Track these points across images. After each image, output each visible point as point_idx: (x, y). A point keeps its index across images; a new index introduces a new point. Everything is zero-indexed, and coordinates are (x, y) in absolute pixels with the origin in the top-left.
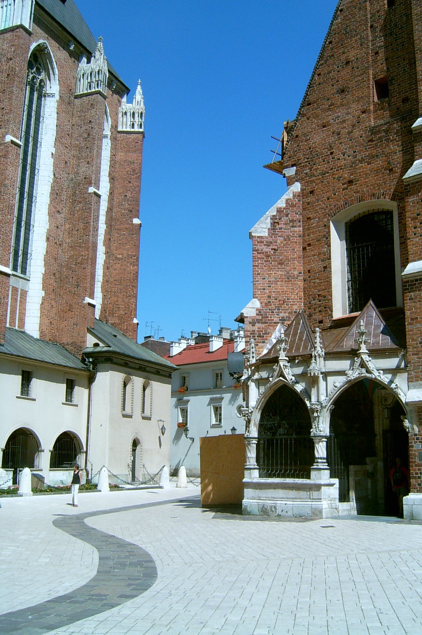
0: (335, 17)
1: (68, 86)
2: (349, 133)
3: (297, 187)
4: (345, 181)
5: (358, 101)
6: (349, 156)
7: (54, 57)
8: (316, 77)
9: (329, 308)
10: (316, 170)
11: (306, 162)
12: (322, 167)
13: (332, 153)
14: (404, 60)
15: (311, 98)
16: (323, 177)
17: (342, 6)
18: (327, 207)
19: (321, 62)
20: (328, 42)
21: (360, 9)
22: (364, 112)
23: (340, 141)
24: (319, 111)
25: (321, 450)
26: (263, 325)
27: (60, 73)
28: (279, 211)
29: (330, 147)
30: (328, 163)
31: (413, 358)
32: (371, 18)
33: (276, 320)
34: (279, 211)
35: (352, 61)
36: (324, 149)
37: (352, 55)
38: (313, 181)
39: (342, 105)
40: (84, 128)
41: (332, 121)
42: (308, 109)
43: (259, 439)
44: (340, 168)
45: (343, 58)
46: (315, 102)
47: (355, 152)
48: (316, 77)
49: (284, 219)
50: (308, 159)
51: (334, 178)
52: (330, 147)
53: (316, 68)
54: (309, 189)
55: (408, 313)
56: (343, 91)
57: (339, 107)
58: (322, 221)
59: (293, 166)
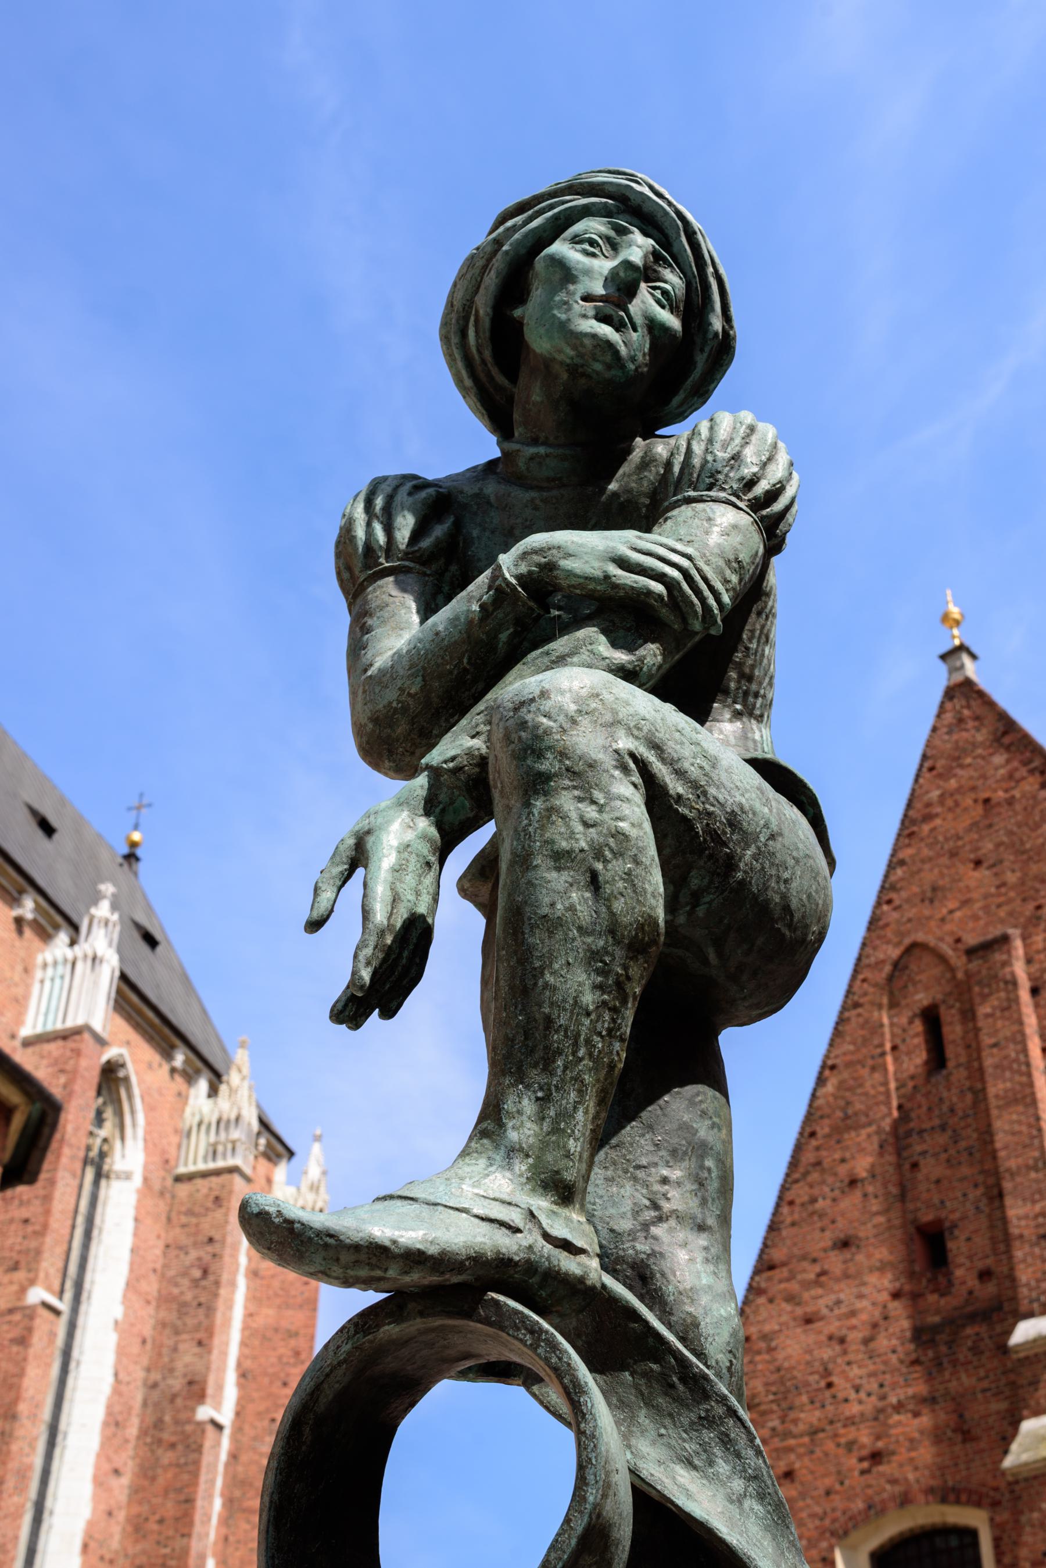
0: (821, 1081)
1: (164, 1152)
2: (867, 1341)
4: (865, 1452)
6: (869, 1395)
7: (139, 1084)
8: (785, 1210)
10: (795, 1421)
11: (772, 1402)
12: (810, 1417)
13: (830, 1385)
14: (976, 1186)
15: (777, 1255)
16: (812, 1440)
17: (837, 1057)
18: (825, 1513)
19: (796, 1176)
20: (807, 1133)
21: (873, 1069)
23: (847, 1359)
24: (794, 1286)
27: (148, 1123)
29: (826, 1369)
30: (823, 1406)
32: (898, 1089)
35: (863, 1180)
36: (812, 1373)
38: (790, 1449)
39: (846, 1276)
40: (194, 1254)
41: (825, 1311)
42: (769, 1279)
44: (850, 1421)
45: (843, 1170)
46: (784, 1264)
47: (881, 1386)
48: (785, 1210)
50: (775, 1394)
51: (838, 1445)
52: (826, 1369)
53: (784, 1189)
54: (782, 1466)
56: (844, 1244)
57: (838, 1280)
58: (815, 1546)
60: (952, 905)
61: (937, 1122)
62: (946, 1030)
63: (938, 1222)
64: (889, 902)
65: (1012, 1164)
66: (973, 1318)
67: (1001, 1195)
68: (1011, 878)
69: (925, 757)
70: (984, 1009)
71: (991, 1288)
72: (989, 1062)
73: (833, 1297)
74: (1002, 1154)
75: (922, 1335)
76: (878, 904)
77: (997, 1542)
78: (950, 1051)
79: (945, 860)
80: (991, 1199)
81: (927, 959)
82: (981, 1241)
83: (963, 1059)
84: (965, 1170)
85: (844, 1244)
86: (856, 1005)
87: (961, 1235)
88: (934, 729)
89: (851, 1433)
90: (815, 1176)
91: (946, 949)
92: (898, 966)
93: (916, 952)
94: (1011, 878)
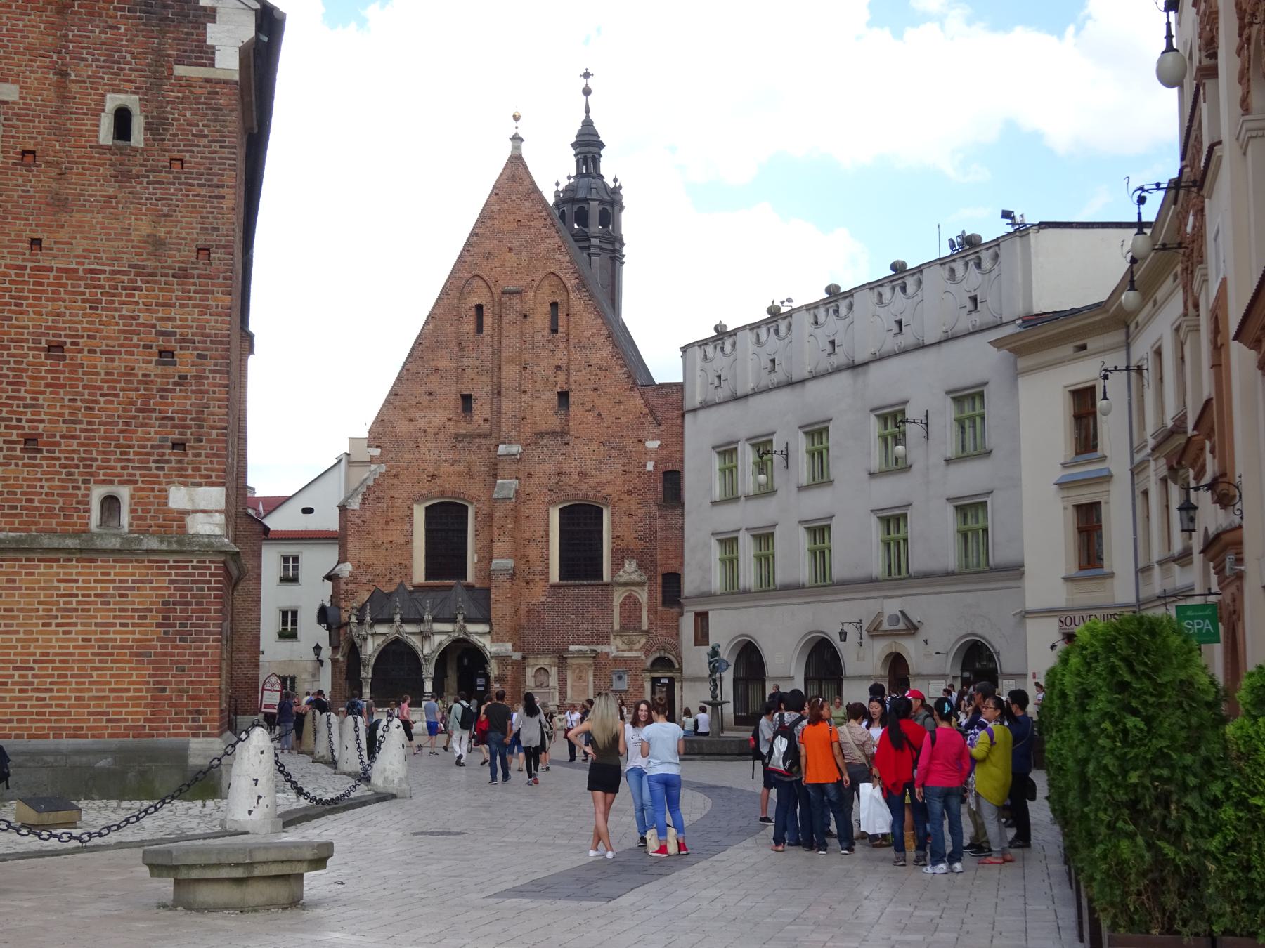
0: (427, 322)
2: (435, 434)
3: (383, 468)
5: (445, 408)
9: (409, 575)
12: (408, 457)
22: (450, 419)
25: (428, 687)
26: (354, 586)
28: (369, 488)
31: (496, 628)
33: (364, 581)
34: (369, 488)
37: (442, 364)
43: (372, 679)
49: (372, 496)
53: (405, 364)
54: (394, 472)
55: (492, 596)
56: (430, 394)
59: (377, 447)
60: (496, 264)
61: (475, 355)
62: (485, 318)
63: (470, 396)
64: (468, 251)
65: (507, 385)
66: (479, 436)
67: (499, 393)
68: (524, 263)
69: (495, 187)
70: (505, 320)
71: (487, 426)
72: (504, 341)
73: (423, 414)
74: (503, 381)
75: (456, 438)
76: (463, 250)
77: (477, 513)
78: (485, 327)
79: (496, 242)
80: (493, 394)
81: (481, 283)
82: (487, 408)
83: (490, 333)
84: (484, 378)
85: (430, 394)
86: (448, 294)
87: (480, 402)
88: (501, 175)
89: (425, 466)
90: (420, 362)
91: (490, 283)
92: (468, 282)
93: (477, 278)
94: (524, 263)
